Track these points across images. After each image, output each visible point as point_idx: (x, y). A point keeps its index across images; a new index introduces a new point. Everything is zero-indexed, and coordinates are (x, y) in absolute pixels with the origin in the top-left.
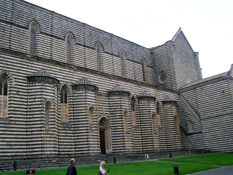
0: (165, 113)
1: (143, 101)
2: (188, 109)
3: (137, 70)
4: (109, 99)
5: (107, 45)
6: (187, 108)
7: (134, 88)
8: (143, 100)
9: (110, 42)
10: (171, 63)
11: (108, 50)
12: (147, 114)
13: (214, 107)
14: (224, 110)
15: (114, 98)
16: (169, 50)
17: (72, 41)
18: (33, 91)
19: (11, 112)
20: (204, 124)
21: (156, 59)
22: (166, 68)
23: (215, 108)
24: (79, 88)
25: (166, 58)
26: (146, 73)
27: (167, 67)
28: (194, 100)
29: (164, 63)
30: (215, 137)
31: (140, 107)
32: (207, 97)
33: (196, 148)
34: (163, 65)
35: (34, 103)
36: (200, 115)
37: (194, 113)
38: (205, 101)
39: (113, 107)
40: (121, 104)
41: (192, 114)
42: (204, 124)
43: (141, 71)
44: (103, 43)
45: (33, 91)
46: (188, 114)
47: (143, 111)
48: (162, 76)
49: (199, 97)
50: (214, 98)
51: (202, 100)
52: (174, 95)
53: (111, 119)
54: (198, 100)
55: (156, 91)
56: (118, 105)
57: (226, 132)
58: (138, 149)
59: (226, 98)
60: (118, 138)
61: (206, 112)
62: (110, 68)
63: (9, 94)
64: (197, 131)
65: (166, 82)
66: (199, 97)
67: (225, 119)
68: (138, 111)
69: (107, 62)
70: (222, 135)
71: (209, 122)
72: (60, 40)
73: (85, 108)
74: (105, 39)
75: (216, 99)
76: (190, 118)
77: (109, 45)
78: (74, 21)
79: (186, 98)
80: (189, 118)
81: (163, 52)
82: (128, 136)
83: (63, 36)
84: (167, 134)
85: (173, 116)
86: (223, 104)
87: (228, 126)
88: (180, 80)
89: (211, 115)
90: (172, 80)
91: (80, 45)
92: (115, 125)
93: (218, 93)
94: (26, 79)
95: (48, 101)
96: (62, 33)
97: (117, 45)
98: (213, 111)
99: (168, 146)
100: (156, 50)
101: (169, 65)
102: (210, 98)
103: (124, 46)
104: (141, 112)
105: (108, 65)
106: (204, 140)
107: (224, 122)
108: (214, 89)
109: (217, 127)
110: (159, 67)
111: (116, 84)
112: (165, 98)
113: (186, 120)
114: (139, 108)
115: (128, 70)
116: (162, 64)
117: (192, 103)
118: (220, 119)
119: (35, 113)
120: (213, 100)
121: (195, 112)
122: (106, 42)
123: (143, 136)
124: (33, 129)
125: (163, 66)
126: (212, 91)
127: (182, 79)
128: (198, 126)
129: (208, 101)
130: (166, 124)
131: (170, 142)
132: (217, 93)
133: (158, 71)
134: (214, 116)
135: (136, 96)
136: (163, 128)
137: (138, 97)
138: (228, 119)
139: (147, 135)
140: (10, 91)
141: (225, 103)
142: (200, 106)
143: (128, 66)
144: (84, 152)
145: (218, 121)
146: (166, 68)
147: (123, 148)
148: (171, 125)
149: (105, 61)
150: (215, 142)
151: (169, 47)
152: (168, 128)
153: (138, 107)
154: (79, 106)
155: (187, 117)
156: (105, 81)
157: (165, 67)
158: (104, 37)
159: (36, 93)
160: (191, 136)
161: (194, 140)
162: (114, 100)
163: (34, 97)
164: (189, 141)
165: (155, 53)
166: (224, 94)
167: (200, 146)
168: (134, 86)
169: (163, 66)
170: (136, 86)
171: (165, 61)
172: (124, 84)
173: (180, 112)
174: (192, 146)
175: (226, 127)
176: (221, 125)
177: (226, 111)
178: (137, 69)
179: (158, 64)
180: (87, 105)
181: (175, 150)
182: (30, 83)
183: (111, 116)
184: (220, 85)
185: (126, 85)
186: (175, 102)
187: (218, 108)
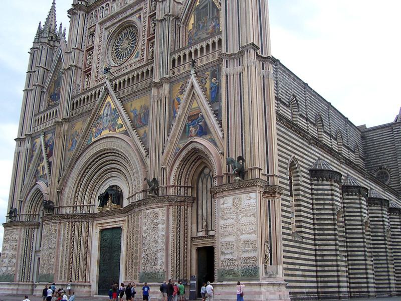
1: (393, 215)
8: (392, 214)
15: (373, 208)
16: (397, 137)
18: (320, 192)
19: (302, 224)
27: (391, 162)
29: (385, 156)
34: (383, 158)
35: (323, 212)
45: (320, 192)
48: (379, 175)
60: (382, 270)
63: (296, 195)
72: (285, 108)
73: (360, 223)
78: (296, 79)
91: (303, 117)
92: (377, 250)
94: (308, 172)
96: (287, 97)
100: (372, 133)
110: (376, 160)
119: (326, 227)
124: (325, 253)
140: (296, 190)
144: (363, 290)
154: (352, 218)
157: (386, 161)
159: (326, 197)
162: (374, 211)
163: (322, 202)
169: (382, 159)
171: (387, 153)
180: (363, 218)
182: (315, 180)
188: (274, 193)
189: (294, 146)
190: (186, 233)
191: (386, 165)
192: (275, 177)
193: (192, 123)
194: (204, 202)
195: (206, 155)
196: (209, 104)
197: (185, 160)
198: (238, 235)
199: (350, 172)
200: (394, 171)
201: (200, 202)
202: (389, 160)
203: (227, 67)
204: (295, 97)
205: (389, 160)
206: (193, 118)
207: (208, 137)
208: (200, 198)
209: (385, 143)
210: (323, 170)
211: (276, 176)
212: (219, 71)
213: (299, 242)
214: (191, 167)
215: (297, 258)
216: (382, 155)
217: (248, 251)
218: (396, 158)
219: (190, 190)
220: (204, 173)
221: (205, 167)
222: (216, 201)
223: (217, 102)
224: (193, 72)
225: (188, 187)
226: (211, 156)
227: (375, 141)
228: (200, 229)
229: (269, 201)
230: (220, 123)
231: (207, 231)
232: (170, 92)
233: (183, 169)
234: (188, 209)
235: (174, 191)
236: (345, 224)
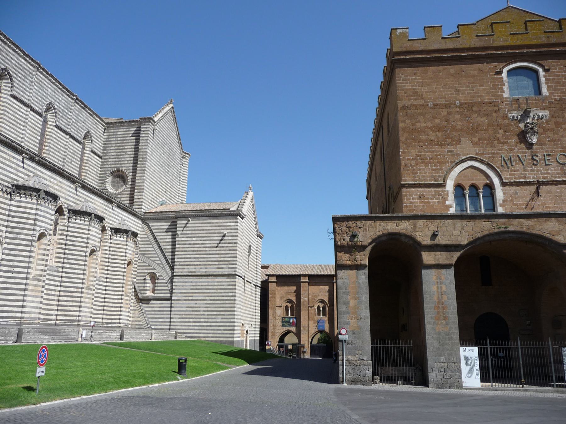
0: (113, 251)
2: (154, 252)
3: (70, 153)
4: (11, 200)
5: (23, 82)
6: (153, 249)
7: (66, 189)
9: (30, 79)
11: (22, 93)
12: (82, 247)
13: (204, 258)
14: (220, 266)
20: (179, 284)
21: (113, 142)
22: (128, 165)
26: (86, 163)
30: (193, 311)
31: (70, 229)
32: (194, 237)
33: (153, 325)
34: (124, 158)
38: (190, 244)
39: (16, 220)
40: (37, 217)
41: (160, 262)
42: (179, 284)
43: (78, 157)
44: (15, 76)
46: (152, 261)
47: (74, 239)
51: (185, 241)
52: (134, 221)
53: (6, 243)
55: (106, 206)
56: (30, 216)
58: (47, 315)
59: (227, 247)
62: (15, 132)
65: (123, 191)
67: (217, 282)
68: (64, 237)
69: (13, 118)
71: (189, 282)
74: (20, 67)
75: (210, 245)
76: (154, 269)
77: (25, 83)
82: (36, 285)
84: (107, 292)
85: (125, 260)
87: (220, 295)
88: (150, 195)
89: (194, 270)
97: (43, 90)
98: (200, 265)
99: (104, 317)
102: (201, 240)
103: (57, 96)
104: (70, 241)
105: (13, 124)
111: (33, 173)
112: (117, 221)
114: (67, 231)
115: (53, 148)
116: (122, 156)
117: (164, 242)
120: (205, 246)
122: (22, 74)
123: (62, 289)
126: (206, 230)
127: (154, 194)
130: (109, 272)
131: (109, 309)
132: (213, 235)
133: (110, 166)
134: (199, 274)
135: (66, 206)
136: (103, 279)
137: (69, 210)
139: (72, 289)
143: (55, 140)
145: (206, 284)
147: (20, 309)
148: (119, 275)
149: (10, 116)
150: (191, 320)
151: (145, 129)
152: (112, 281)
153: (66, 228)
155: (149, 266)
156: (12, 159)
157: (126, 162)
158: (18, 63)
161: (154, 311)
167: (162, 324)
168: (67, 186)
169: (123, 159)
170: (70, 187)
172: (49, 176)
173: (137, 254)
175: (218, 296)
176: (208, 291)
177: (222, 268)
178: (72, 151)
179: (113, 154)
183: (6, 237)
185: (52, 180)
186: (135, 235)
187: (210, 261)
191: (125, 167)
209: (129, 141)
216: (123, 155)
227: (119, 136)
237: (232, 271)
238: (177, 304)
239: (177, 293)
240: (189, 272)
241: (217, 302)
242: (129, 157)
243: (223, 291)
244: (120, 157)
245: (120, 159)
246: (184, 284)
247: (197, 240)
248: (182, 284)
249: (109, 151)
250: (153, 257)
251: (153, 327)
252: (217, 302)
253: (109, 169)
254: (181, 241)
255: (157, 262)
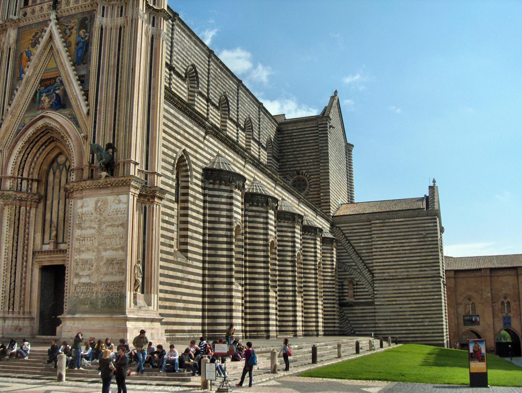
1: (307, 235)
2: (349, 257)
6: (347, 254)
8: (307, 233)
10: (322, 161)
14: (422, 269)
15: (283, 224)
16: (322, 135)
17: (192, 85)
20: (381, 289)
21: (288, 144)
22: (308, 167)
23: (405, 263)
24: (257, 201)
25: (310, 148)
27: (312, 167)
28: (364, 243)
29: (305, 158)
30: (398, 315)
32: (392, 240)
34: (303, 160)
36: (374, 272)
37: (361, 266)
38: (387, 247)
41: (356, 267)
42: (381, 289)
46: (348, 266)
48: (295, 181)
49: (377, 237)
50: (406, 244)
54: (373, 243)
57: (421, 309)
59: (428, 248)
61: (386, 267)
64: (363, 301)
66: (377, 237)
67: (421, 285)
70: (412, 313)
71: (391, 286)
72: (180, 81)
76: (352, 274)
79: (346, 235)
80: (348, 275)
81: (307, 136)
83: (183, 72)
86: (421, 258)
87: (425, 298)
89: (395, 274)
90: (322, 194)
91: (203, 96)
93: (414, 237)
94: (201, 171)
95: (238, 223)
96: (183, 66)
98: (401, 268)
101: (319, 165)
102: (399, 243)
106: (377, 318)
107: (419, 290)
108: (408, 228)
109: (405, 298)
110: (293, 163)
113: (343, 277)
116: (300, 159)
117: (358, 246)
118: (413, 284)
121: (363, 264)
125: (303, 163)
126: (404, 232)
128: (367, 291)
129: (394, 249)
132: (411, 237)
133: (288, 169)
134: (401, 277)
138: (428, 286)
141: (424, 256)
142: (375, 255)
145: (409, 287)
146: (308, 167)
150: (397, 325)
151: (323, 129)
155: (345, 271)
157: (306, 164)
160: (351, 308)
161: (357, 317)
163: (217, 213)
164: (345, 317)
165: (286, 132)
166: (424, 241)
169: (302, 162)
171: (308, 155)
174: (349, 327)
176: (412, 295)
177: (425, 271)
179: (290, 157)
181: (333, 333)
182: (211, 183)
184: (419, 224)
188: (153, 197)
189: (187, 135)
190: (26, 245)
191: (305, 169)
192: (156, 176)
193: (46, 90)
194: (55, 202)
195: (63, 137)
196: (73, 65)
197: (31, 142)
198: (99, 251)
199: (258, 176)
200: (315, 178)
201: (49, 202)
202: (309, 164)
203: (103, 16)
204: (193, 66)
205: (309, 164)
206: (48, 83)
207: (66, 112)
208: (49, 196)
209: (306, 142)
210: (221, 171)
211: (159, 175)
212: (91, 20)
213: (183, 264)
214: (39, 152)
215: (179, 286)
216: (301, 157)
217: (112, 273)
218: (318, 161)
219: (35, 185)
220: (58, 163)
221: (60, 154)
222: (72, 203)
223: (84, 64)
224: (53, 16)
225: (32, 180)
226: (70, 140)
227: (294, 137)
228: (47, 240)
229: (145, 208)
230: (86, 94)
231: (57, 243)
232: (17, 41)
233: (28, 154)
234: (32, 212)
235: (11, 184)
236: (246, 244)
237: (435, 273)
238: (380, 309)
239: (379, 298)
240: (390, 276)
241: (423, 305)
242: (308, 159)
243: (428, 294)
244: (298, 159)
245: (299, 162)
246: (386, 288)
247: (394, 243)
248: (383, 288)
249: (286, 154)
250: (348, 262)
251: (357, 333)
252: (423, 305)
253: (288, 172)
254: (378, 244)
255: (353, 267)
